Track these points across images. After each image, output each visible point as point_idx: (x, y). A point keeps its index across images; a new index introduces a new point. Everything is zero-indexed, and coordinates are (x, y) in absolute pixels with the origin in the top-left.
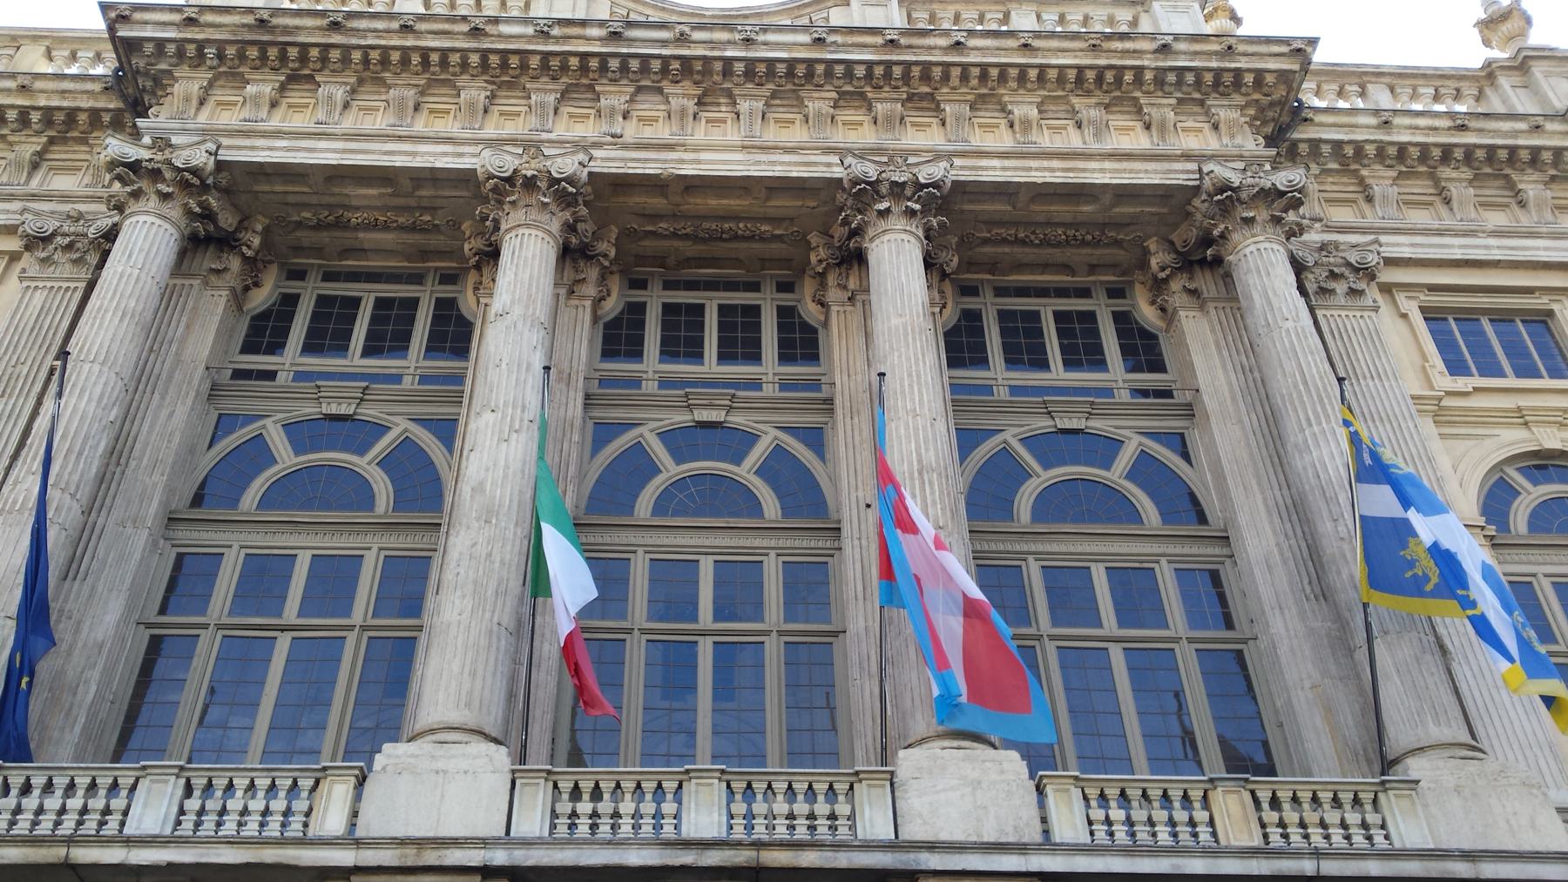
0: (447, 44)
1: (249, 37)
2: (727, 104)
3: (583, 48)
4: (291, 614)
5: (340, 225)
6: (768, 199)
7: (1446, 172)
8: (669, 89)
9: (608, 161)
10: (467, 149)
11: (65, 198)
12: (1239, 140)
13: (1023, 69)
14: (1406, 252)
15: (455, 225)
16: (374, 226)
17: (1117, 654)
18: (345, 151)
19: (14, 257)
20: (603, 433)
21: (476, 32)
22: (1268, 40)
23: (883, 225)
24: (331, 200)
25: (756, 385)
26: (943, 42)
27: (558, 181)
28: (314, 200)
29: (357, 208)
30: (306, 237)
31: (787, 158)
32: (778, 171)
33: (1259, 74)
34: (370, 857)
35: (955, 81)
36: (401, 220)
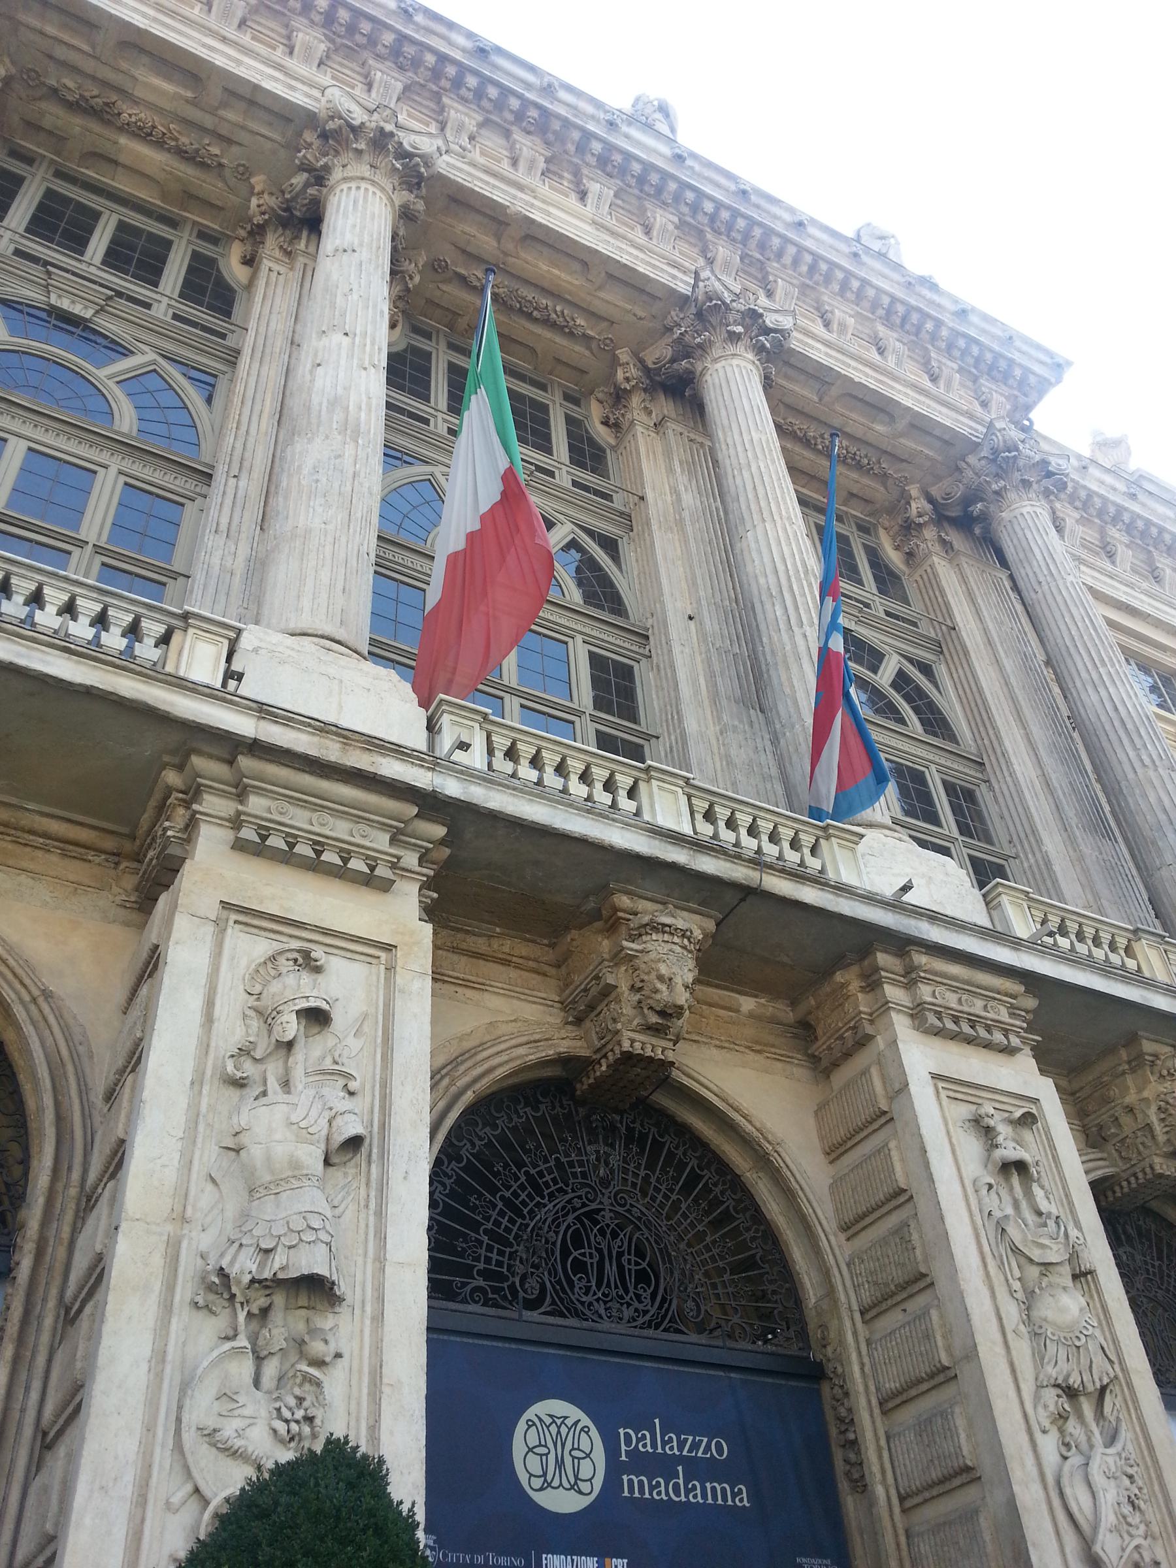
2: (570, 182)
5: (103, 114)
6: (600, 288)
8: (518, 136)
15: (244, 173)
16: (143, 134)
18: (155, 20)
22: (1039, 347)
23: (731, 349)
24: (111, 76)
27: (410, 156)
28: (89, 65)
29: (136, 102)
30: (54, 115)
35: (787, 259)
36: (184, 140)
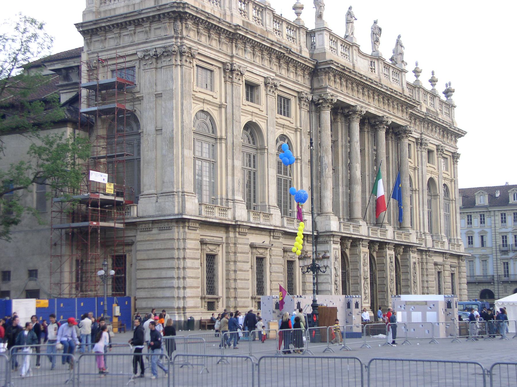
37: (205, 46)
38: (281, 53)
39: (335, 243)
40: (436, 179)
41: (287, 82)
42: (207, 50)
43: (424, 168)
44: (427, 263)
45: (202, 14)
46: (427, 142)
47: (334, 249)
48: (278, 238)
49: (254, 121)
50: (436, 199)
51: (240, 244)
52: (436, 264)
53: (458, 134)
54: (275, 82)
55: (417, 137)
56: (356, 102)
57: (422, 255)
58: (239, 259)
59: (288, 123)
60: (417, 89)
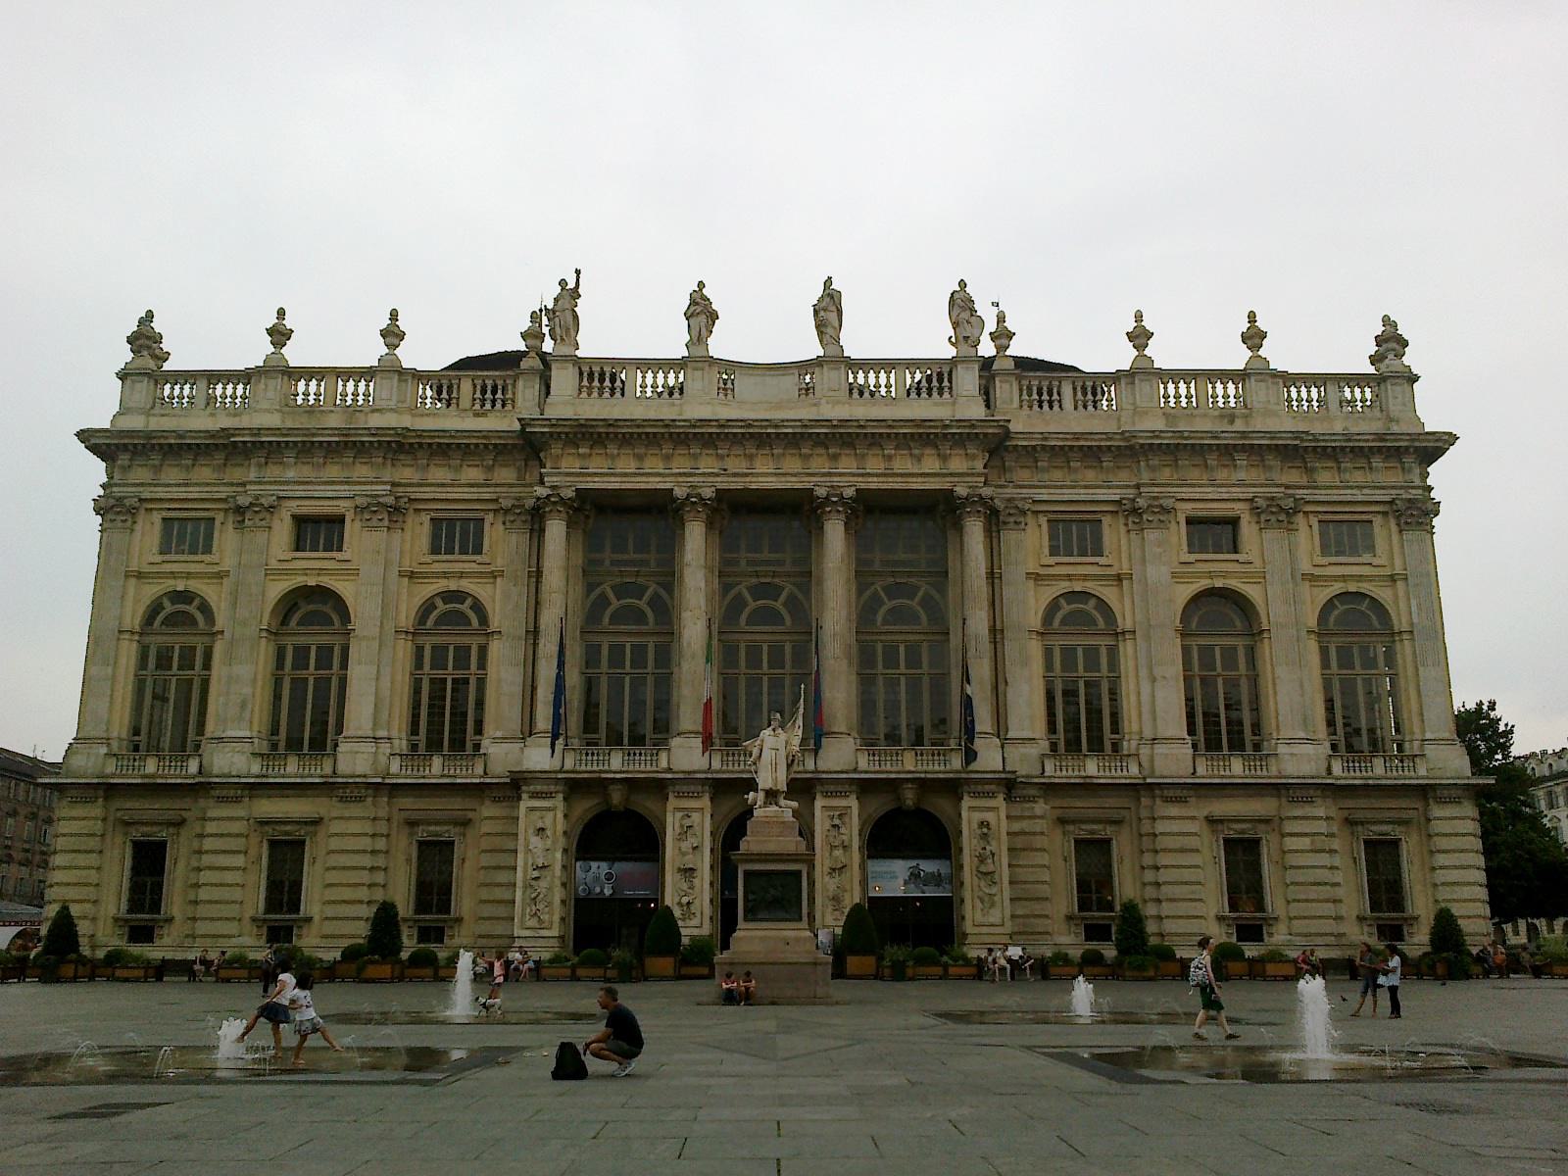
0: (655, 430)
1: (576, 430)
3: (710, 431)
4: (628, 669)
7: (1070, 454)
9: (723, 483)
10: (667, 479)
11: (511, 485)
12: (976, 462)
13: (889, 434)
14: (1045, 497)
17: (903, 680)
19: (495, 511)
20: (726, 588)
21: (667, 426)
25: (780, 563)
26: (855, 424)
31: (794, 479)
32: (789, 486)
33: (985, 434)
34: (677, 776)
37: (169, 485)
38: (389, 442)
39: (535, 795)
40: (1252, 592)
41: (449, 489)
42: (175, 489)
43: (1158, 573)
44: (1154, 819)
45: (133, 437)
46: (1168, 503)
47: (532, 809)
48: (360, 799)
49: (312, 582)
50: (1262, 640)
51: (214, 819)
52: (1212, 821)
53: (1435, 446)
54: (381, 500)
55: (1117, 498)
56: (681, 479)
57: (1139, 799)
58: (206, 847)
59: (473, 565)
60: (1123, 382)
